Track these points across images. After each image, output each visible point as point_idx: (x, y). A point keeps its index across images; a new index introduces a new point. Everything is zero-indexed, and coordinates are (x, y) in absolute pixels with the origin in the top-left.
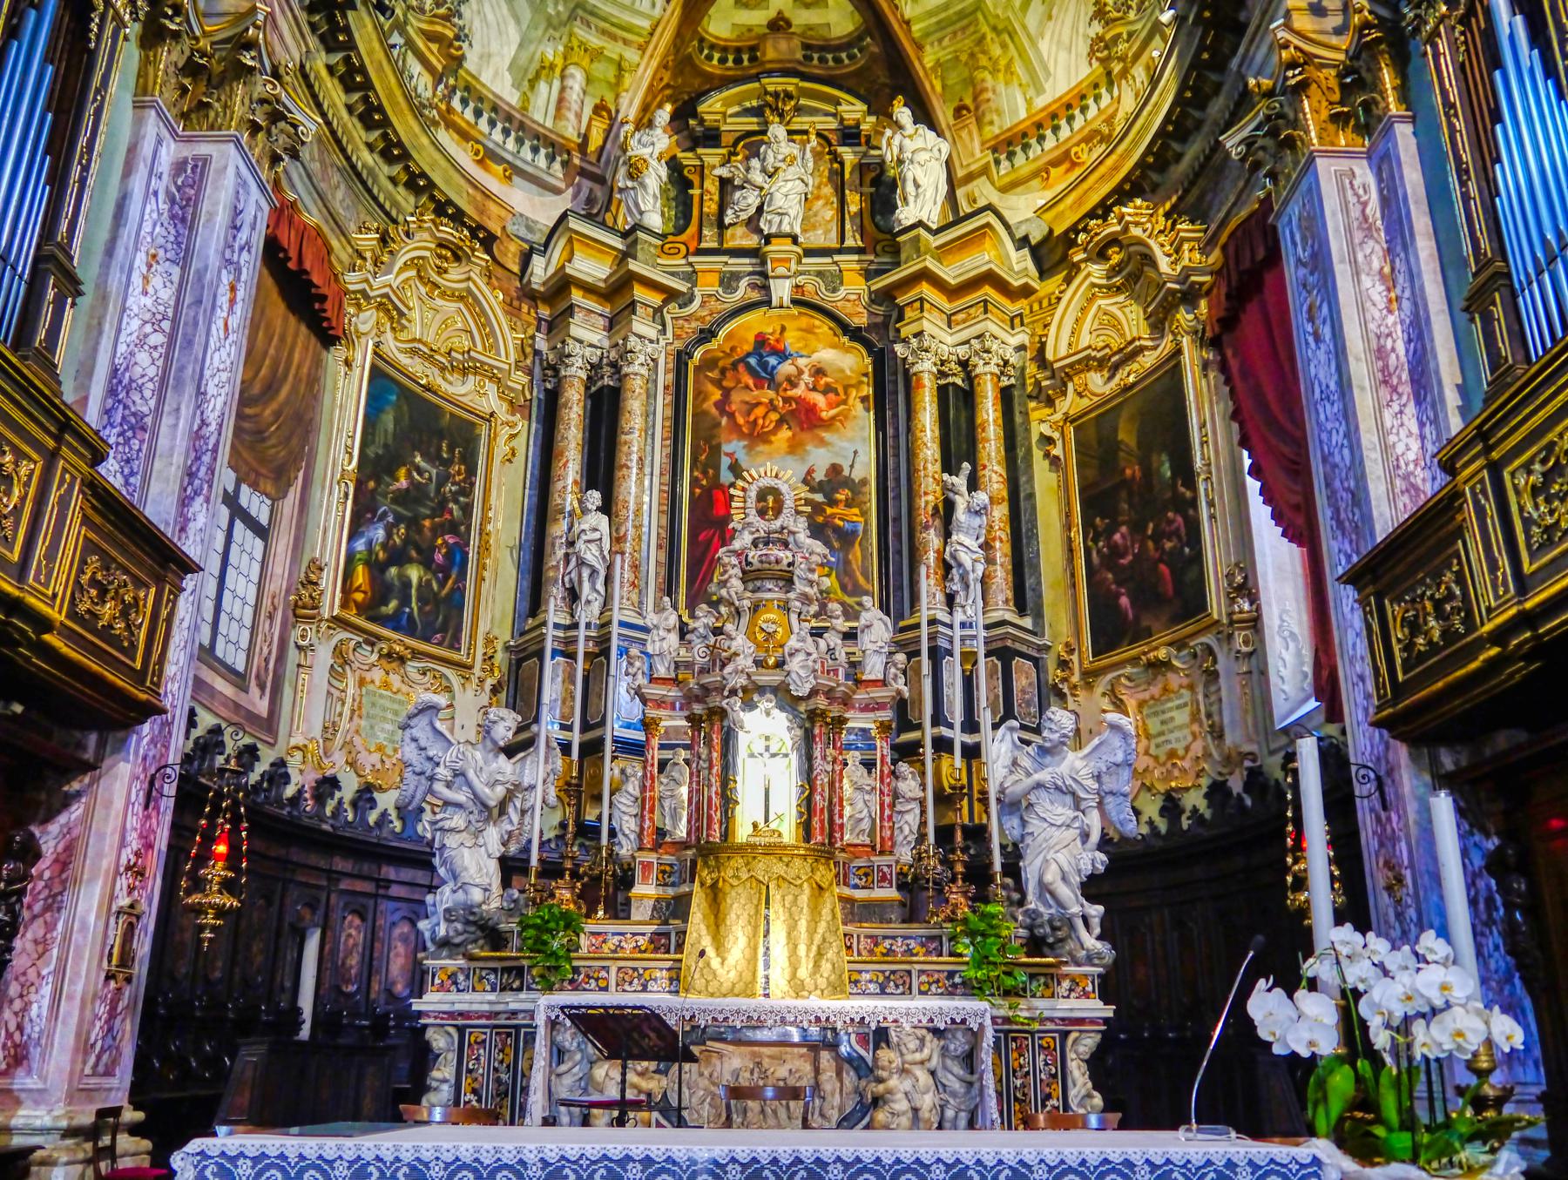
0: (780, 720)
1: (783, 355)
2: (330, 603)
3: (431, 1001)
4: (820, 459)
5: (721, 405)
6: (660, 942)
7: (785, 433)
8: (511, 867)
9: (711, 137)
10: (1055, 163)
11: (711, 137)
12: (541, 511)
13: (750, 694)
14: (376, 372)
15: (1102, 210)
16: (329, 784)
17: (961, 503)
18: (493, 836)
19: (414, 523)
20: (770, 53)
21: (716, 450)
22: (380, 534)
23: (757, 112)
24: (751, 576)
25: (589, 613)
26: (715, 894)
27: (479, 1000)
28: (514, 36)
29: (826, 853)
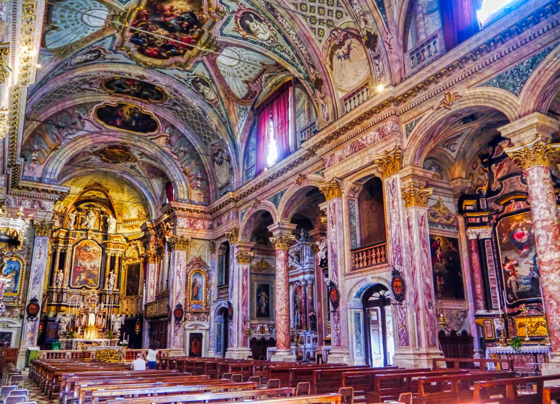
1: (89, 247)
4: (93, 264)
5: (79, 254)
6: (81, 334)
7: (88, 259)
8: (67, 327)
10: (132, 226)
15: (135, 240)
17: (112, 275)
20: (92, 198)
23: (89, 206)
24: (92, 301)
25: (59, 287)
26: (87, 330)
27: (65, 340)
29: (97, 327)
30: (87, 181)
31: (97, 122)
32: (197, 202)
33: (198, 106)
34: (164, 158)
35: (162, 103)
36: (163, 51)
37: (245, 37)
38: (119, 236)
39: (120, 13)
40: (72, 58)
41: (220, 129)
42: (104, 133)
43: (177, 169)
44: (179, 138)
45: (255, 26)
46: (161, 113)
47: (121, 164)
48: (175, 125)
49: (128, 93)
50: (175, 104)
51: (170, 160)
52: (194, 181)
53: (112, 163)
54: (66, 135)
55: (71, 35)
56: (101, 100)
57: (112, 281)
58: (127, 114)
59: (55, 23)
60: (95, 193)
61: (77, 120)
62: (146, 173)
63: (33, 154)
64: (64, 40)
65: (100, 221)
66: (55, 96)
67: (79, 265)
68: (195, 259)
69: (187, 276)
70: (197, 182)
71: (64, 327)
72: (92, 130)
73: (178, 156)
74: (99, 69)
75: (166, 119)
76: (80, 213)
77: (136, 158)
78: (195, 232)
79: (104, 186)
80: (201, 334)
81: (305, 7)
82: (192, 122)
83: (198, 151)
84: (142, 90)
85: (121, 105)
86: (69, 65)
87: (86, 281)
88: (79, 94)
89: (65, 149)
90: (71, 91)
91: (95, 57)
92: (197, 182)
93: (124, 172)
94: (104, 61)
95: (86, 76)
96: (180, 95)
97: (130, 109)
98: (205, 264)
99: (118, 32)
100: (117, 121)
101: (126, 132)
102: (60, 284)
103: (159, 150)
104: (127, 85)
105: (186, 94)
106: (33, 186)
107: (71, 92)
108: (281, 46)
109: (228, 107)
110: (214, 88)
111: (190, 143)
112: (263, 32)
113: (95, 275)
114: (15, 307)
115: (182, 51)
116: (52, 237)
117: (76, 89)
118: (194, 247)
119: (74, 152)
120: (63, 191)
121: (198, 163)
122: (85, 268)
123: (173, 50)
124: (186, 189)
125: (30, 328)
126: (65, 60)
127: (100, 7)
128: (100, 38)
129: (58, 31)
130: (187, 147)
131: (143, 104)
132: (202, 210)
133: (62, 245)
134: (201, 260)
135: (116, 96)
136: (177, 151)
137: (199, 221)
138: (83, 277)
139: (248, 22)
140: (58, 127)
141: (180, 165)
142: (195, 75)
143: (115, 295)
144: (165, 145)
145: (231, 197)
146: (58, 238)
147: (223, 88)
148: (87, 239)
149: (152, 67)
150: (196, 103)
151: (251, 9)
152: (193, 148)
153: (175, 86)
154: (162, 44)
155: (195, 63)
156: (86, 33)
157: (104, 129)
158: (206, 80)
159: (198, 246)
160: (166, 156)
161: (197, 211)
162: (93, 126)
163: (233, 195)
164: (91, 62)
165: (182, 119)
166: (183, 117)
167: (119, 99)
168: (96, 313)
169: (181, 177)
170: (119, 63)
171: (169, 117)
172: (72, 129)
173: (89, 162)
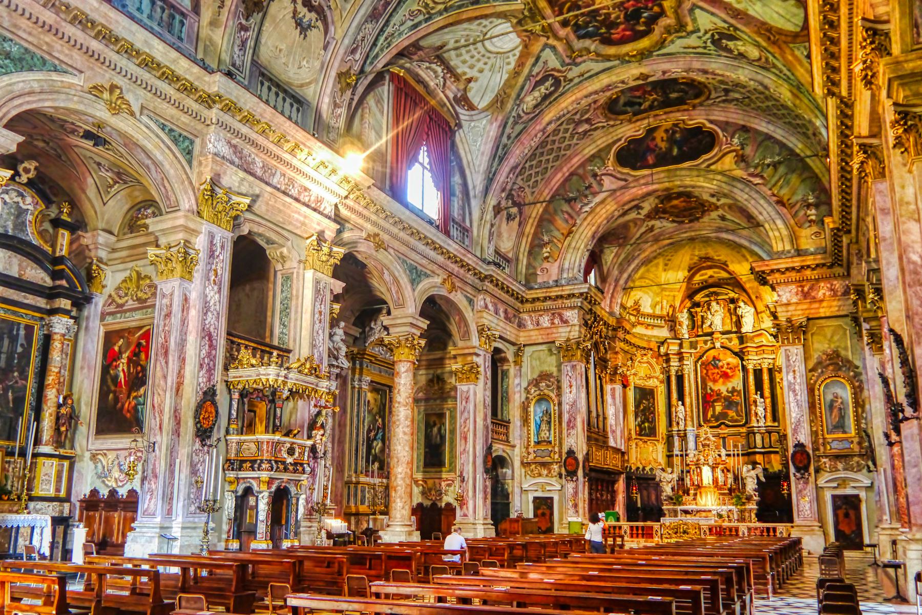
0: (709, 468)
1: (720, 360)
2: (634, 436)
3: (664, 507)
4: (730, 386)
5: (706, 374)
8: (673, 489)
9: (697, 305)
11: (697, 305)
12: (669, 405)
13: (704, 464)
14: (635, 387)
16: (638, 468)
18: (670, 485)
19: (645, 415)
20: (711, 281)
21: (706, 385)
22: (639, 419)
23: (707, 296)
24: (703, 446)
25: (682, 427)
28: (650, 300)
30: (685, 258)
31: (619, 172)
32: (812, 250)
33: (750, 79)
34: (735, 190)
35: (708, 98)
36: (635, 25)
38: (761, 334)
39: (523, 13)
40: (519, 105)
41: (798, 102)
42: (632, 185)
43: (762, 202)
44: (760, 145)
46: (719, 115)
47: (706, 219)
48: (748, 124)
49: (651, 108)
50: (727, 91)
51: (747, 190)
52: (801, 213)
53: (691, 221)
54: (581, 209)
55: (493, 77)
56: (620, 136)
57: (760, 411)
58: (663, 140)
59: (465, 74)
60: (710, 272)
61: (592, 180)
62: (745, 220)
63: (545, 250)
64: (490, 88)
65: (731, 314)
66: (548, 160)
67: (709, 391)
68: (824, 357)
69: (811, 390)
70: (809, 212)
71: (667, 490)
72: (614, 187)
73: (762, 177)
74: (574, 98)
75: (731, 120)
76: (699, 310)
77: (713, 204)
78: (816, 305)
79: (716, 258)
80: (857, 496)
82: (768, 106)
83: (802, 155)
84: (665, 94)
85: (651, 131)
86: (522, 114)
87: (723, 415)
88: (583, 141)
89: (581, 230)
90: (567, 143)
91: (551, 86)
92: (809, 212)
93: (720, 230)
94: (572, 84)
95: (564, 115)
96: (713, 73)
97: (666, 131)
98: (848, 361)
99: (548, 38)
100: (649, 158)
101: (663, 171)
102: (682, 424)
103: (724, 179)
104: (639, 97)
105: (719, 69)
106: (544, 295)
107: (570, 145)
109: (783, 57)
110: (746, 37)
111: (783, 146)
113: (737, 404)
114: (551, 463)
115: (656, 9)
116: (660, 355)
117: (572, 136)
118: (819, 334)
119: (594, 228)
120: (582, 291)
121: (804, 176)
122: (719, 394)
123: (645, 15)
124: (785, 232)
125: (571, 491)
126: (510, 112)
127: (491, 23)
128: (531, 60)
129: (476, 80)
130: (779, 155)
131: (686, 113)
132: (817, 262)
133: (677, 364)
134: (838, 356)
135: (637, 121)
136: (759, 169)
137: (822, 284)
138: (719, 408)
140: (569, 201)
141: (769, 192)
142: (706, 32)
143: (770, 433)
144: (735, 167)
145: (831, 226)
146: (667, 355)
147: (756, 29)
148: (714, 348)
149: (644, 55)
150: (743, 74)
152: (792, 152)
153: (697, 65)
154: (622, 16)
155: (690, 15)
156: (508, 64)
157: (630, 179)
158: (726, 32)
159: (828, 332)
160: (739, 185)
161: (808, 266)
162: (614, 180)
163: (834, 222)
164: (556, 95)
165: (753, 109)
166: (753, 106)
167: (646, 121)
168: (711, 463)
169: (773, 213)
170: (597, 74)
171: (735, 116)
172: (586, 196)
173: (656, 232)
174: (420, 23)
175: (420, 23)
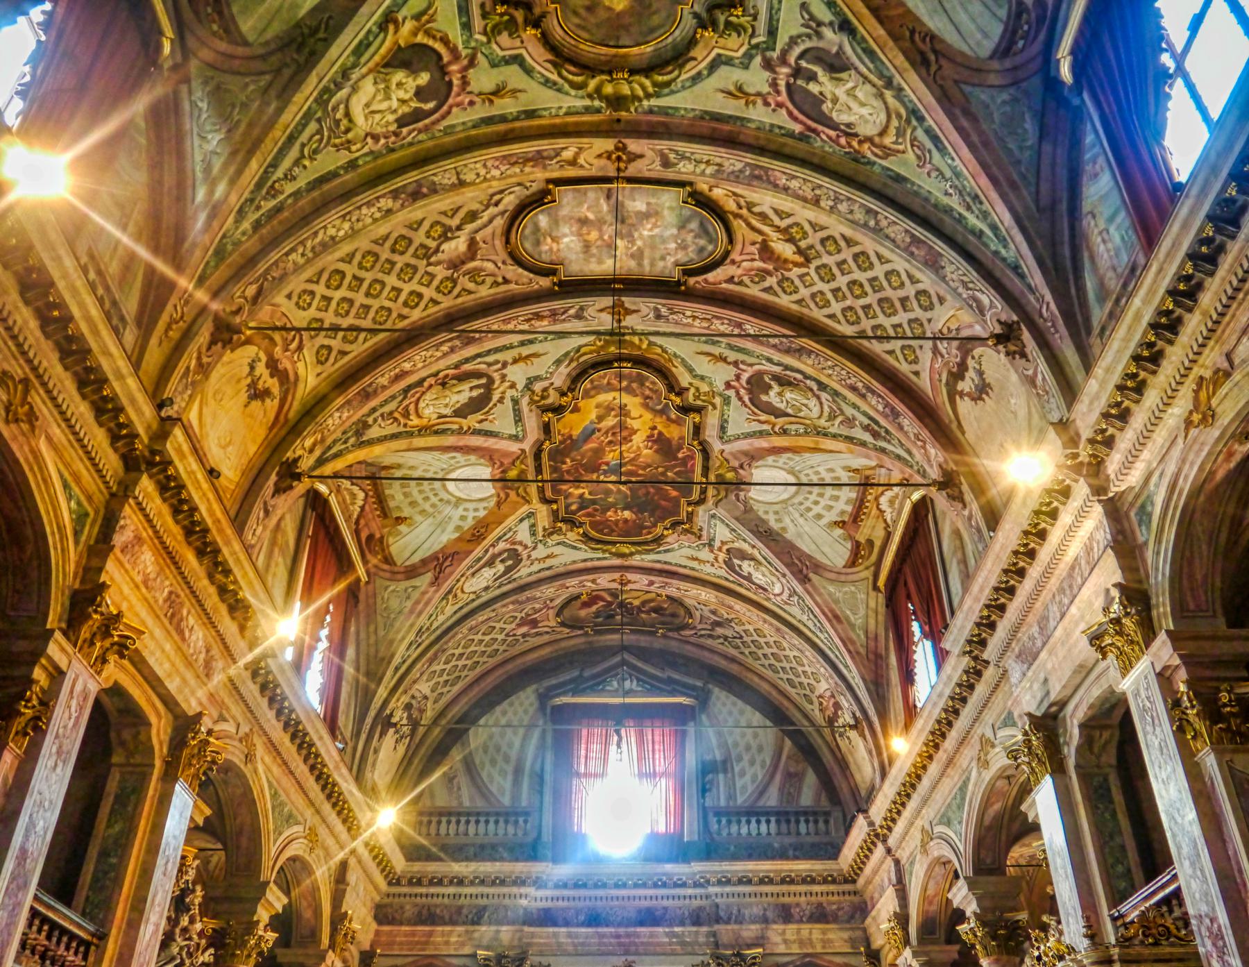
37: (391, 28)
45: (402, 94)
81: (368, 265)
108: (316, 152)
112: (374, 107)
139: (424, 78)
151: (443, 117)
174: (928, 132)
175: (928, 132)
